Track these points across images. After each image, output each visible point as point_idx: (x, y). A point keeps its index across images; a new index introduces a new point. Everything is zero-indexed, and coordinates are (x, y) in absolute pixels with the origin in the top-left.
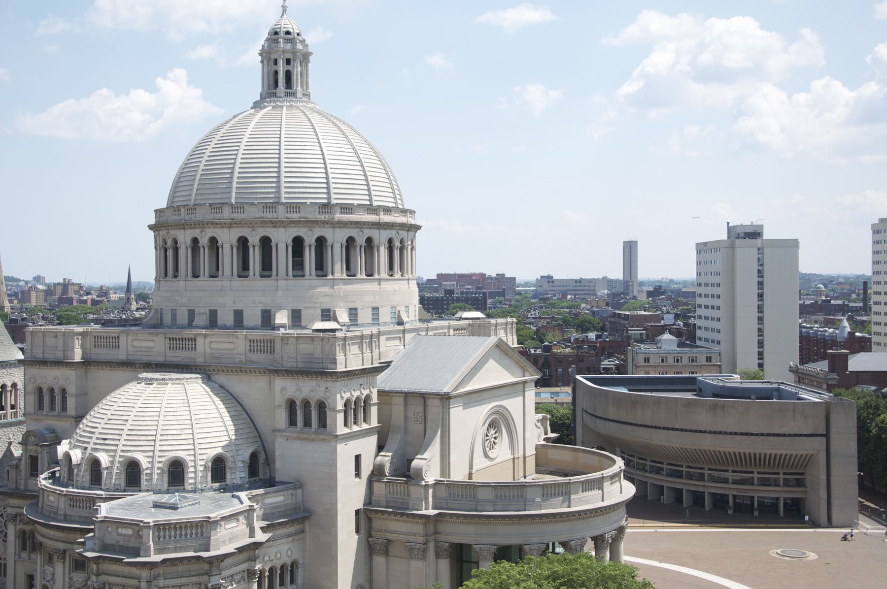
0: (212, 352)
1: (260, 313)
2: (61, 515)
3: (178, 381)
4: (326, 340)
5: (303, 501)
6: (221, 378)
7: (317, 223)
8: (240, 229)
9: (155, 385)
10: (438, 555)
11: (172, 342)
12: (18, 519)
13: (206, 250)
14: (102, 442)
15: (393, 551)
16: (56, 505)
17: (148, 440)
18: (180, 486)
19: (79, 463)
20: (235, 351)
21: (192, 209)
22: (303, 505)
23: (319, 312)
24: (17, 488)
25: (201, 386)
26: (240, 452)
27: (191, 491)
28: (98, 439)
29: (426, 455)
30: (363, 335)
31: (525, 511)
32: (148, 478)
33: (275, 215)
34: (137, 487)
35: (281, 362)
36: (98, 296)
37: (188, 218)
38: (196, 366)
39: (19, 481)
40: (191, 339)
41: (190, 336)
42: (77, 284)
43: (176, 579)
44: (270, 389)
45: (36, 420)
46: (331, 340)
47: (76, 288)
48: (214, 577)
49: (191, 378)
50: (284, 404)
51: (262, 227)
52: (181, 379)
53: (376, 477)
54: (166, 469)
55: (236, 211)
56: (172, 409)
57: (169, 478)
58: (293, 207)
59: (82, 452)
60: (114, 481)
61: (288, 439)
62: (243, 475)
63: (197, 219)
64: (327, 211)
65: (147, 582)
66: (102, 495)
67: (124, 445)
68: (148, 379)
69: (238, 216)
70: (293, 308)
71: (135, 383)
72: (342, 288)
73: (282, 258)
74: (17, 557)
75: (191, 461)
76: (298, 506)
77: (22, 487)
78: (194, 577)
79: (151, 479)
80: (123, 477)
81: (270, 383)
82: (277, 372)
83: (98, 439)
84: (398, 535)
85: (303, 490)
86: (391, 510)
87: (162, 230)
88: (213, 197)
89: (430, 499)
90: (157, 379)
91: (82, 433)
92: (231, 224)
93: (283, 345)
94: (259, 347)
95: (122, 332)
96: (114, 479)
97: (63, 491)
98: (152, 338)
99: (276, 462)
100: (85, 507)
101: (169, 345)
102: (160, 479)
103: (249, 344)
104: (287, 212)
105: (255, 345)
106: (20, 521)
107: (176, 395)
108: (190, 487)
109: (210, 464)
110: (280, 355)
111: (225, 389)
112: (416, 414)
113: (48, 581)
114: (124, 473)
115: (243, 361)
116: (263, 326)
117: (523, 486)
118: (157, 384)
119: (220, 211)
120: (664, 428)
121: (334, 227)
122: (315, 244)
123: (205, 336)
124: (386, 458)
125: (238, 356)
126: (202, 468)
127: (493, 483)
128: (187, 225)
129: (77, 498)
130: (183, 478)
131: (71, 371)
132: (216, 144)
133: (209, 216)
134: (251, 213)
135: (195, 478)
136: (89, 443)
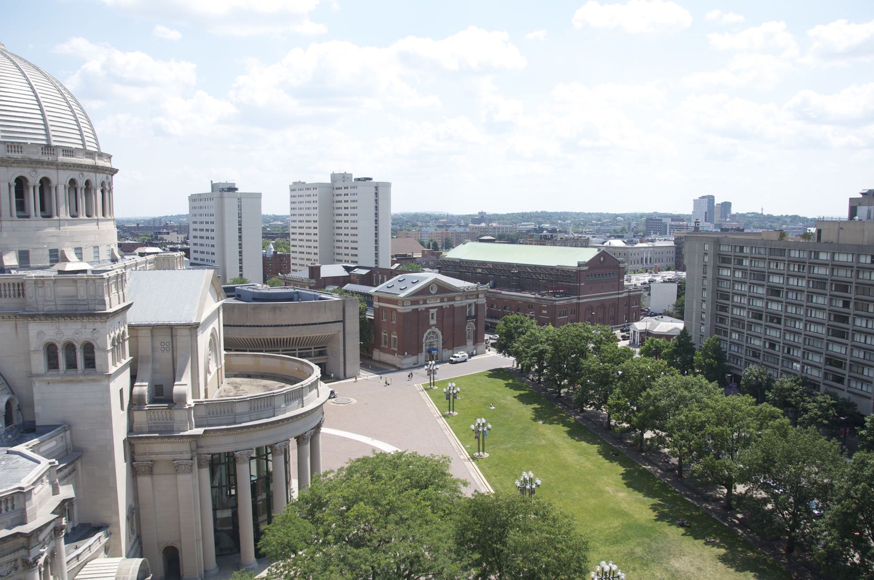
5: (72, 442)
7: (42, 164)
10: (200, 466)
15: (156, 470)
22: (73, 446)
23: (48, 253)
29: (183, 381)
31: (274, 416)
35: (36, 306)
44: (17, 333)
46: (97, 281)
50: (42, 349)
58: (15, 146)
64: (49, 152)
70: (20, 249)
72: (68, 229)
76: (69, 447)
81: (16, 327)
82: (33, 317)
84: (163, 456)
86: (157, 435)
89: (193, 420)
93: (37, 288)
104: (8, 151)
110: (34, 299)
112: (163, 344)
117: (272, 397)
120: (237, 326)
121: (58, 169)
122: (15, 184)
124: (143, 388)
127: (248, 398)
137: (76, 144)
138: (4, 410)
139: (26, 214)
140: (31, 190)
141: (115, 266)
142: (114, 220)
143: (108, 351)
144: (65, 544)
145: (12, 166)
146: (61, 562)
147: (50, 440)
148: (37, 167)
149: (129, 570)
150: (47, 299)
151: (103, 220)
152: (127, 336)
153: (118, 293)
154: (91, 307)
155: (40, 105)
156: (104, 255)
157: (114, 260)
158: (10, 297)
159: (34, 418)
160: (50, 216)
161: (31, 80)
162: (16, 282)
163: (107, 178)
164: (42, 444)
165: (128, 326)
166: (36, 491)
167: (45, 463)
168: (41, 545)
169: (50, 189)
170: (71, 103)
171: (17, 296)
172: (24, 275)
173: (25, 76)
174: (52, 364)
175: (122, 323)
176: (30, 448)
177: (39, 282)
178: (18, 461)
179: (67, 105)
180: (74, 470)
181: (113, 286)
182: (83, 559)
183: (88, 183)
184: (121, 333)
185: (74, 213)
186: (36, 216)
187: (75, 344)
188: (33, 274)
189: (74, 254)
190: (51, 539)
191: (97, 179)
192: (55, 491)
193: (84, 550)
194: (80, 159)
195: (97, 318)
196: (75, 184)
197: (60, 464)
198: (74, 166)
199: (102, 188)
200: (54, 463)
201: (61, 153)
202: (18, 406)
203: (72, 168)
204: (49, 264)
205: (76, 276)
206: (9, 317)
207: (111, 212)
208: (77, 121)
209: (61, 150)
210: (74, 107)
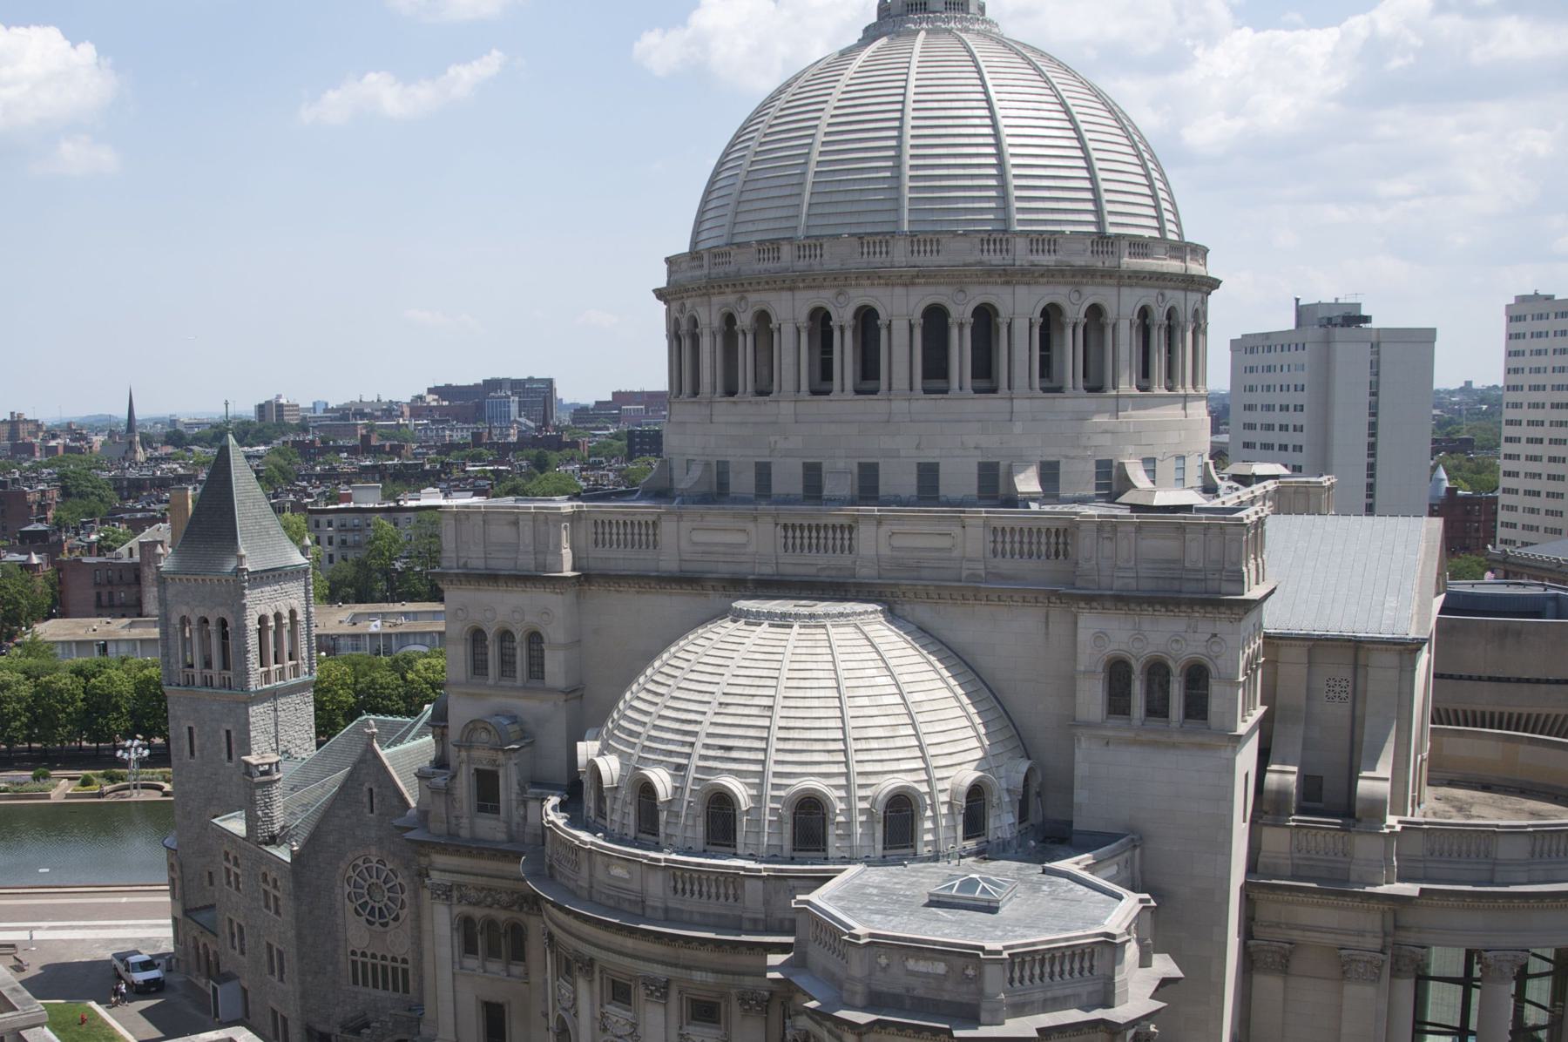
8: (931, 289)
13: (848, 335)
14: (720, 753)
24: (453, 835)
39: (453, 821)
57: (885, 831)
59: (671, 775)
67: (777, 762)
69: (927, 260)
73: (1020, 350)
77: (464, 833)
79: (849, 835)
114: (790, 821)
119: (884, 249)
130: (913, 830)
133: (857, 261)
134: (956, 253)
135: (935, 831)
139: (1054, 385)
140: (1069, 332)
145: (1037, 283)
148: (1081, 284)
183: (1171, 314)
186: (1074, 388)
194: (1160, 262)
201: (1127, 253)
203: (1146, 282)
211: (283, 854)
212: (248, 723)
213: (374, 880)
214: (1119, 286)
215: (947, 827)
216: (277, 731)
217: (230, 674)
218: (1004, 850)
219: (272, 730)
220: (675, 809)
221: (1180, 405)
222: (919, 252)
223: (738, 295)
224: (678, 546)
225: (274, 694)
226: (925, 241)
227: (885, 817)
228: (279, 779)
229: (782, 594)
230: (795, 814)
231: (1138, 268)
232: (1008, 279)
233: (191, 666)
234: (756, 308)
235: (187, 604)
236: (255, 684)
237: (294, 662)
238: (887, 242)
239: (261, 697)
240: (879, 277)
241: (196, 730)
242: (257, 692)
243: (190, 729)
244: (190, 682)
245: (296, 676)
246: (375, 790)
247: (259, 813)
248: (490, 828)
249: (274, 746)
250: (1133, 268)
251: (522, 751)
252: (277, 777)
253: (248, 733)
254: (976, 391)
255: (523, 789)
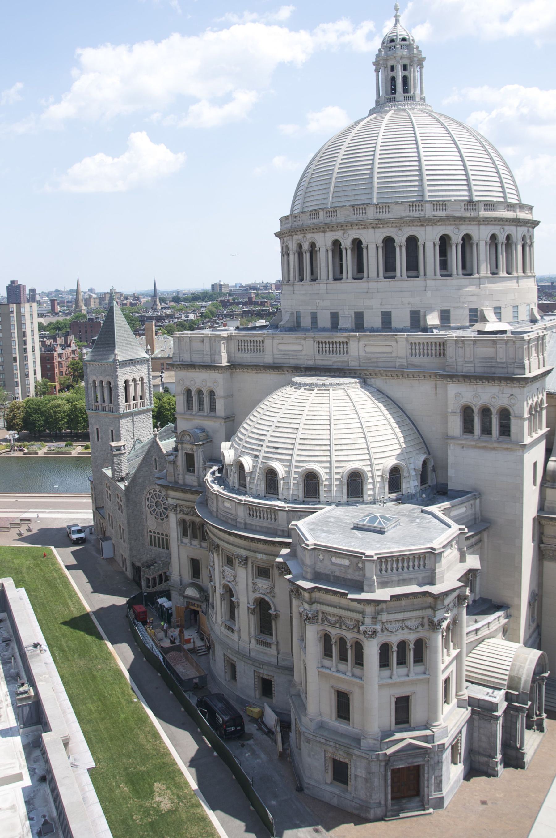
0: (367, 355)
1: (408, 315)
2: (240, 523)
3: (338, 387)
4: (511, 343)
6: (379, 382)
7: (464, 221)
8: (386, 229)
9: (316, 391)
11: (321, 345)
12: (178, 509)
14: (273, 450)
16: (233, 512)
17: (322, 450)
18: (359, 497)
19: (251, 471)
20: (394, 355)
21: (333, 211)
24: (176, 482)
25: (361, 391)
26: (412, 460)
27: (370, 503)
28: (268, 447)
30: (539, 336)
32: (326, 489)
33: (422, 214)
34: (316, 498)
35: (455, 367)
36: (133, 300)
37: (328, 220)
38: (350, 370)
39: (176, 476)
40: (343, 342)
41: (341, 340)
42: (119, 293)
43: (399, 614)
44: (436, 393)
45: (187, 419)
46: (518, 343)
47: (118, 295)
48: (439, 611)
49: (350, 383)
50: (458, 411)
51: (409, 226)
52: (341, 384)
53: (550, 483)
54: (345, 481)
55: (381, 210)
56: (341, 417)
58: (440, 204)
59: (253, 460)
60: (291, 492)
61: (463, 447)
62: (416, 484)
63: (338, 221)
65: (372, 618)
66: (285, 507)
67: (298, 455)
68: (307, 384)
69: (383, 216)
70: (442, 308)
71: (288, 388)
74: (180, 542)
75: (368, 471)
76: (477, 516)
77: (181, 482)
78: (418, 612)
79: (330, 491)
80: (301, 488)
81: (436, 388)
82: (452, 377)
83: (268, 447)
85: (481, 499)
87: (296, 234)
88: (352, 198)
90: (317, 385)
91: (248, 440)
92: (377, 224)
93: (457, 348)
94: (421, 351)
95: (268, 336)
96: (291, 490)
97: (241, 500)
98: (299, 341)
99: (449, 470)
100: (266, 518)
101: (318, 349)
102: (340, 490)
103: (410, 347)
104: (434, 210)
105: (417, 348)
106: (180, 511)
107: (341, 401)
108: (369, 498)
109: (388, 475)
110: (454, 359)
111: (383, 394)
113: (229, 582)
115: (404, 365)
116: (411, 328)
118: (318, 390)
119: (364, 212)
123: (359, 339)
125: (398, 360)
126: (379, 479)
128: (328, 227)
129: (257, 508)
130: (362, 489)
131: (219, 375)
132: (347, 147)
133: (352, 218)
134: (397, 212)
135: (374, 489)
136: (260, 451)
137: (496, 197)
138: (421, 469)
139: (449, 273)
141: (535, 327)
142: (534, 277)
143: (524, 419)
144: (467, 615)
145: (436, 225)
146: (461, 631)
147: (460, 506)
148: (459, 224)
149: (526, 659)
150: (466, 359)
151: (523, 277)
152: (545, 405)
153: (538, 356)
154: (510, 370)
155: (463, 160)
156: (524, 316)
157: (534, 321)
158: (432, 356)
159: (447, 481)
160: (471, 274)
161: (454, 136)
162: (438, 341)
163: (528, 231)
164: (452, 509)
165: (547, 394)
166: (445, 554)
167: (455, 529)
168: (445, 609)
169: (471, 246)
170: (492, 154)
171: (438, 356)
172: (446, 335)
173: (449, 133)
174: (468, 428)
175: (540, 390)
176: (442, 511)
177: (460, 342)
178: (430, 522)
179: (488, 157)
180: (480, 541)
181: (533, 349)
182: (481, 634)
183: (508, 237)
184: (539, 401)
185: (495, 270)
186: (457, 274)
187: (492, 408)
188: (454, 334)
189: (493, 314)
190: (454, 606)
191: (518, 233)
192: (462, 559)
193: (483, 626)
195: (515, 382)
196: (496, 239)
197: (469, 531)
198: (495, 221)
199: (523, 242)
200: (464, 529)
201: (483, 208)
202: (433, 466)
204: (468, 324)
205: (496, 337)
206: (430, 376)
207: (532, 269)
208: (498, 172)
209: (483, 205)
210: (495, 158)
211: (122, 486)
212: (119, 427)
213: (158, 500)
214: (479, 225)
215: (380, 488)
216: (133, 430)
217: (112, 405)
218: (412, 499)
219: (131, 430)
220: (253, 476)
221: (515, 281)
222: (380, 212)
223: (302, 235)
224: (273, 353)
225: (132, 414)
226: (382, 207)
227: (348, 483)
228: (125, 453)
229: (327, 374)
230: (304, 480)
231: (488, 216)
232: (422, 223)
233: (97, 402)
234: (310, 241)
235: (95, 375)
236: (122, 410)
237: (143, 400)
238: (365, 208)
239: (125, 416)
240: (361, 225)
241: (99, 430)
242: (123, 414)
243: (97, 429)
244: (97, 409)
245: (144, 406)
246: (157, 459)
247: (116, 468)
248: (191, 479)
249: (132, 437)
250: (486, 216)
251: (205, 445)
252: (123, 452)
253: (119, 431)
254: (408, 277)
255: (205, 463)
